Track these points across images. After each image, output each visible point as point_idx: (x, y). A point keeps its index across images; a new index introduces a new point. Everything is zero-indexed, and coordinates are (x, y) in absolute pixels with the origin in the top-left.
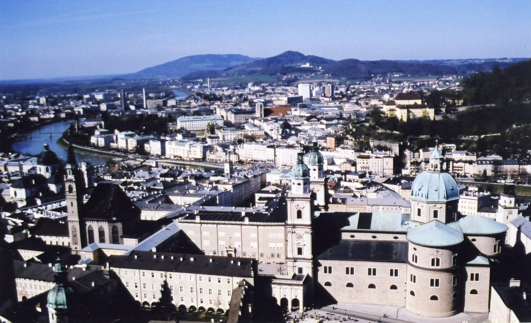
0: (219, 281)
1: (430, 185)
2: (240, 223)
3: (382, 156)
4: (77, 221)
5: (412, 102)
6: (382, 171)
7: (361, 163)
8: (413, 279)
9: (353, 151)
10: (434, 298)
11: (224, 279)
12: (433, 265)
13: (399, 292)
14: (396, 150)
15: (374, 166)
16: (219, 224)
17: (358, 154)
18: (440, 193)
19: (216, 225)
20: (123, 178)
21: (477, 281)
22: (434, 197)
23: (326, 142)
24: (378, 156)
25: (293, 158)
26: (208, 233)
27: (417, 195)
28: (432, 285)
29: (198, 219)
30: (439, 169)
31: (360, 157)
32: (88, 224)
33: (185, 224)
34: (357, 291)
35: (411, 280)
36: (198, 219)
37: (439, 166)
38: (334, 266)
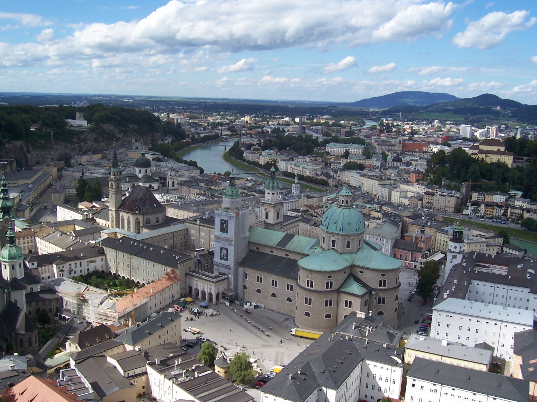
1: (332, 217)
3: (446, 194)
5: (495, 148)
7: (426, 199)
10: (307, 314)
12: (308, 286)
14: (463, 191)
15: (437, 203)
19: (209, 229)
20: (213, 186)
22: (332, 228)
23: (409, 177)
25: (374, 187)
28: (306, 303)
29: (198, 222)
30: (344, 204)
32: (121, 214)
34: (264, 297)
36: (198, 222)
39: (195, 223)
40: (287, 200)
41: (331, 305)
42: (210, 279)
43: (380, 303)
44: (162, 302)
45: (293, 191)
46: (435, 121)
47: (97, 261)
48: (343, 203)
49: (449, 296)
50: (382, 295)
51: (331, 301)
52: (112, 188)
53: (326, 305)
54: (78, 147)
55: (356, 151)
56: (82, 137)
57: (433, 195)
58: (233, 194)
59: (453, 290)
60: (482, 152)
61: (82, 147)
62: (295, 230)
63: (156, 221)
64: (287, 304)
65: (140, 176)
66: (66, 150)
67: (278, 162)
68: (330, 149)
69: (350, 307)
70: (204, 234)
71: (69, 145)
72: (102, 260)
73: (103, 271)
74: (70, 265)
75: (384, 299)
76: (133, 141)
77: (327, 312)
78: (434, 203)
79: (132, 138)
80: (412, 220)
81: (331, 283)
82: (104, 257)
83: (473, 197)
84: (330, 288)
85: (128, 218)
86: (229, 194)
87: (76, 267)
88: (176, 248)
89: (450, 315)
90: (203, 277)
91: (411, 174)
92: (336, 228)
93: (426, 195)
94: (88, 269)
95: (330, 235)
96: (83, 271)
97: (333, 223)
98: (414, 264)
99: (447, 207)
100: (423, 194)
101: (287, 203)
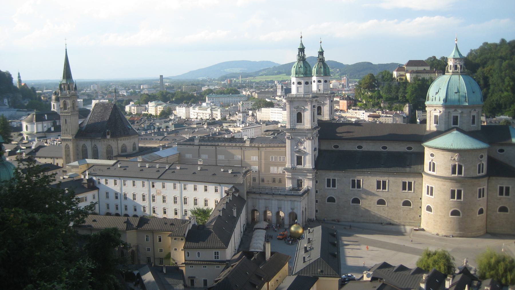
0: (206, 190)
2: (241, 144)
4: (70, 139)
5: (421, 68)
8: (430, 191)
9: (364, 111)
11: (211, 188)
13: (412, 209)
14: (406, 110)
17: (368, 114)
19: (214, 147)
24: (388, 115)
26: (207, 156)
27: (434, 99)
28: (453, 197)
33: (183, 147)
35: (428, 194)
37: (459, 66)
39: (191, 143)
41: (483, 196)
51: (483, 189)
53: (480, 197)
63: (133, 147)
64: (404, 211)
67: (175, 110)
69: (507, 194)
77: (480, 205)
81: (483, 164)
82: (95, 192)
93: (370, 118)
95: (452, 110)
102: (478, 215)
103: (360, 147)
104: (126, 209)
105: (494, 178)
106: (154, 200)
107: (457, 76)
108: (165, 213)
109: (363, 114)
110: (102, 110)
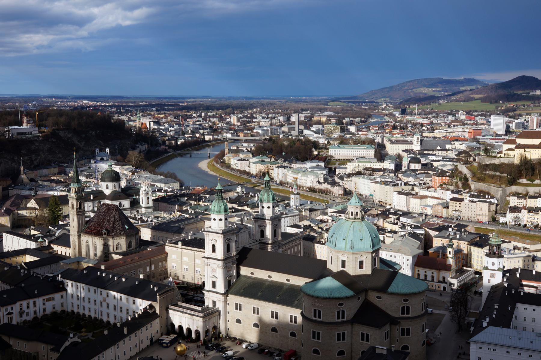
3: (478, 200)
6: (475, 216)
7: (454, 206)
9: (450, 192)
10: (316, 352)
12: (315, 316)
15: (467, 211)
16: (196, 251)
18: (347, 242)
19: (193, 251)
21: (367, 343)
23: (431, 181)
28: (314, 338)
31: (453, 199)
38: (244, 304)
40: (286, 214)
42: (197, 314)
43: (404, 335)
44: (138, 345)
45: (292, 203)
46: (460, 113)
47: (56, 298)
48: (352, 215)
49: (489, 324)
50: (405, 325)
52: (73, 208)
53: (339, 339)
54: (28, 160)
55: (364, 152)
56: (33, 147)
57: (462, 202)
58: (220, 209)
59: (494, 316)
60: (519, 146)
61: (34, 159)
62: (296, 250)
65: (107, 192)
66: (13, 164)
68: (333, 152)
69: (368, 340)
70: (187, 259)
71: (16, 158)
72: (62, 297)
73: (63, 311)
74: (21, 305)
75: (408, 330)
76: (97, 150)
77: (339, 347)
78: (463, 212)
79: (96, 147)
80: (437, 233)
81: (343, 312)
82: (64, 293)
83: (511, 202)
84: (342, 318)
85: (95, 244)
86: (216, 209)
87: (28, 307)
88: (153, 277)
89: (492, 347)
90: (188, 311)
91: (433, 177)
92: (346, 246)
93: (452, 202)
94: (44, 310)
96: (38, 311)
97: (342, 239)
98: (443, 285)
99: (479, 215)
100: (449, 201)
101: (286, 218)
102: (337, 357)
103: (270, 277)
104: (84, 309)
105: (357, 324)
106: (101, 306)
107: (351, 222)
108: (108, 317)
109: (449, 196)
110: (106, 210)
